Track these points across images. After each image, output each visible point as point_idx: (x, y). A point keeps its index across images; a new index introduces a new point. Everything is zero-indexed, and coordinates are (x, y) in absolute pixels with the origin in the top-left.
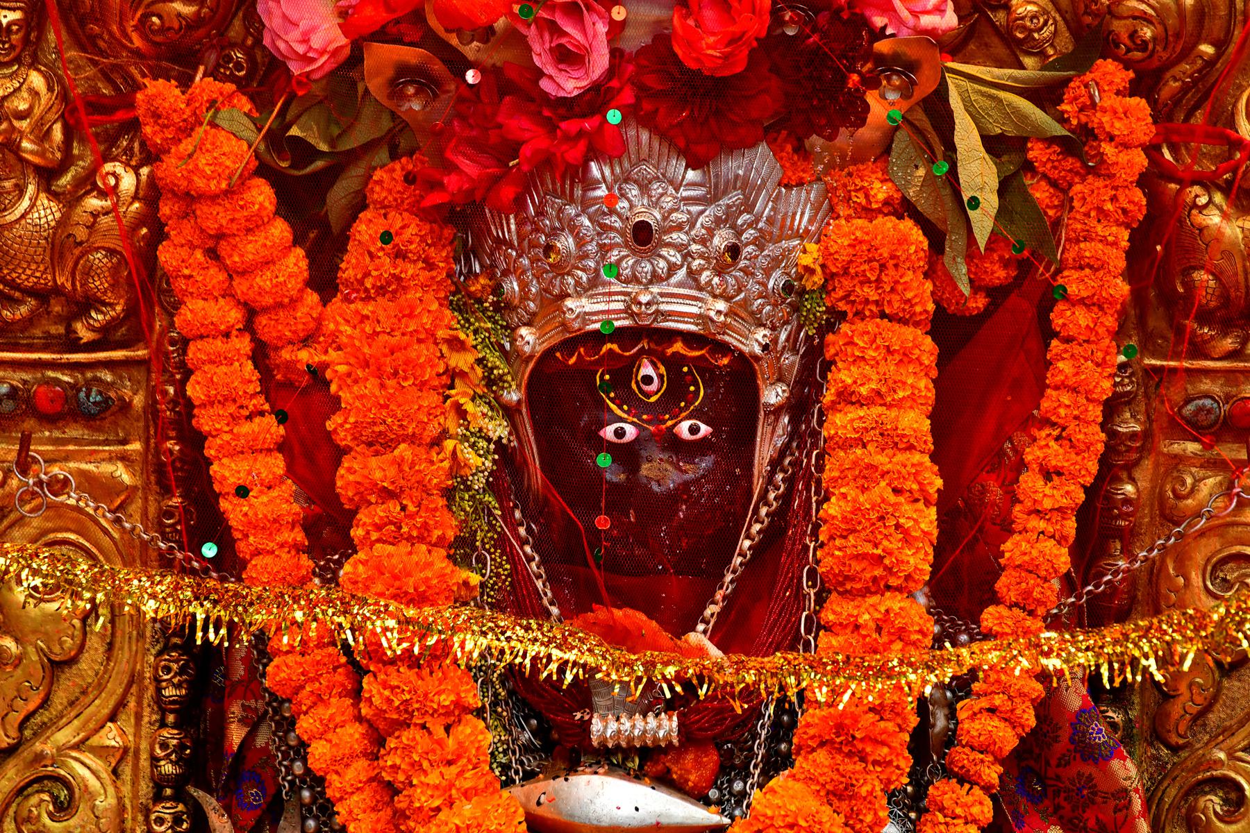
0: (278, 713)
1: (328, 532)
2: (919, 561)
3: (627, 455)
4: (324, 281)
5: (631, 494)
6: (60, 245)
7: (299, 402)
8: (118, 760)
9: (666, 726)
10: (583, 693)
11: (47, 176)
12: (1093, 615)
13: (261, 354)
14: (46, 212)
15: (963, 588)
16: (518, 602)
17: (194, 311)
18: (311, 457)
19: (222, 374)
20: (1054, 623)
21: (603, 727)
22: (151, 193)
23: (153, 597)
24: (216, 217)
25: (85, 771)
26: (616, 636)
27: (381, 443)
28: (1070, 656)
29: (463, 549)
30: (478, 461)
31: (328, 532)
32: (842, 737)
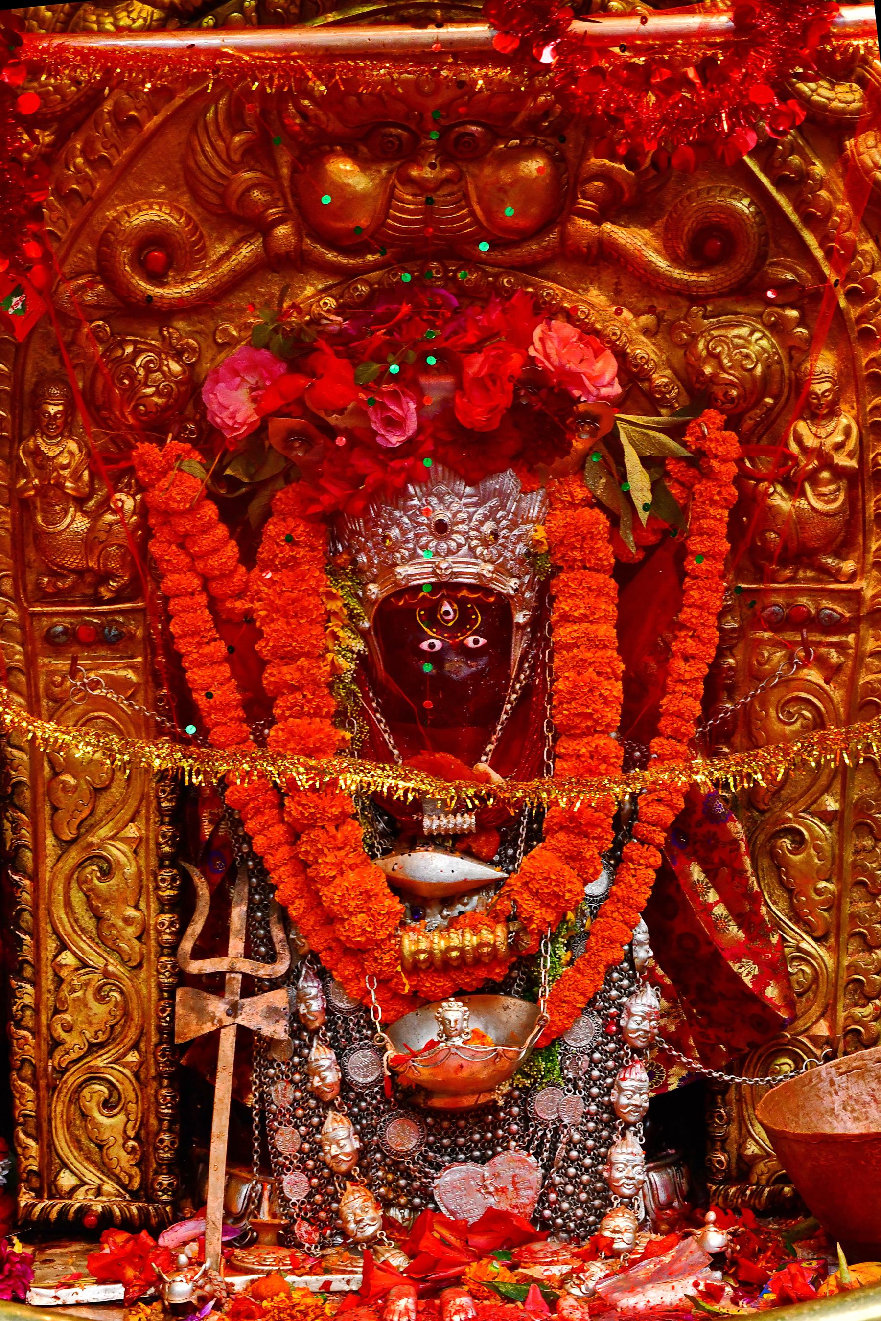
1: (258, 708)
2: (613, 715)
3: (437, 658)
5: (441, 679)
6: (90, 542)
9: (468, 821)
10: (418, 806)
11: (80, 502)
13: (213, 605)
14: (81, 524)
17: (171, 581)
19: (191, 617)
21: (430, 823)
22: (142, 510)
25: (118, 851)
26: (436, 771)
27: (289, 658)
30: (347, 666)
31: (258, 708)
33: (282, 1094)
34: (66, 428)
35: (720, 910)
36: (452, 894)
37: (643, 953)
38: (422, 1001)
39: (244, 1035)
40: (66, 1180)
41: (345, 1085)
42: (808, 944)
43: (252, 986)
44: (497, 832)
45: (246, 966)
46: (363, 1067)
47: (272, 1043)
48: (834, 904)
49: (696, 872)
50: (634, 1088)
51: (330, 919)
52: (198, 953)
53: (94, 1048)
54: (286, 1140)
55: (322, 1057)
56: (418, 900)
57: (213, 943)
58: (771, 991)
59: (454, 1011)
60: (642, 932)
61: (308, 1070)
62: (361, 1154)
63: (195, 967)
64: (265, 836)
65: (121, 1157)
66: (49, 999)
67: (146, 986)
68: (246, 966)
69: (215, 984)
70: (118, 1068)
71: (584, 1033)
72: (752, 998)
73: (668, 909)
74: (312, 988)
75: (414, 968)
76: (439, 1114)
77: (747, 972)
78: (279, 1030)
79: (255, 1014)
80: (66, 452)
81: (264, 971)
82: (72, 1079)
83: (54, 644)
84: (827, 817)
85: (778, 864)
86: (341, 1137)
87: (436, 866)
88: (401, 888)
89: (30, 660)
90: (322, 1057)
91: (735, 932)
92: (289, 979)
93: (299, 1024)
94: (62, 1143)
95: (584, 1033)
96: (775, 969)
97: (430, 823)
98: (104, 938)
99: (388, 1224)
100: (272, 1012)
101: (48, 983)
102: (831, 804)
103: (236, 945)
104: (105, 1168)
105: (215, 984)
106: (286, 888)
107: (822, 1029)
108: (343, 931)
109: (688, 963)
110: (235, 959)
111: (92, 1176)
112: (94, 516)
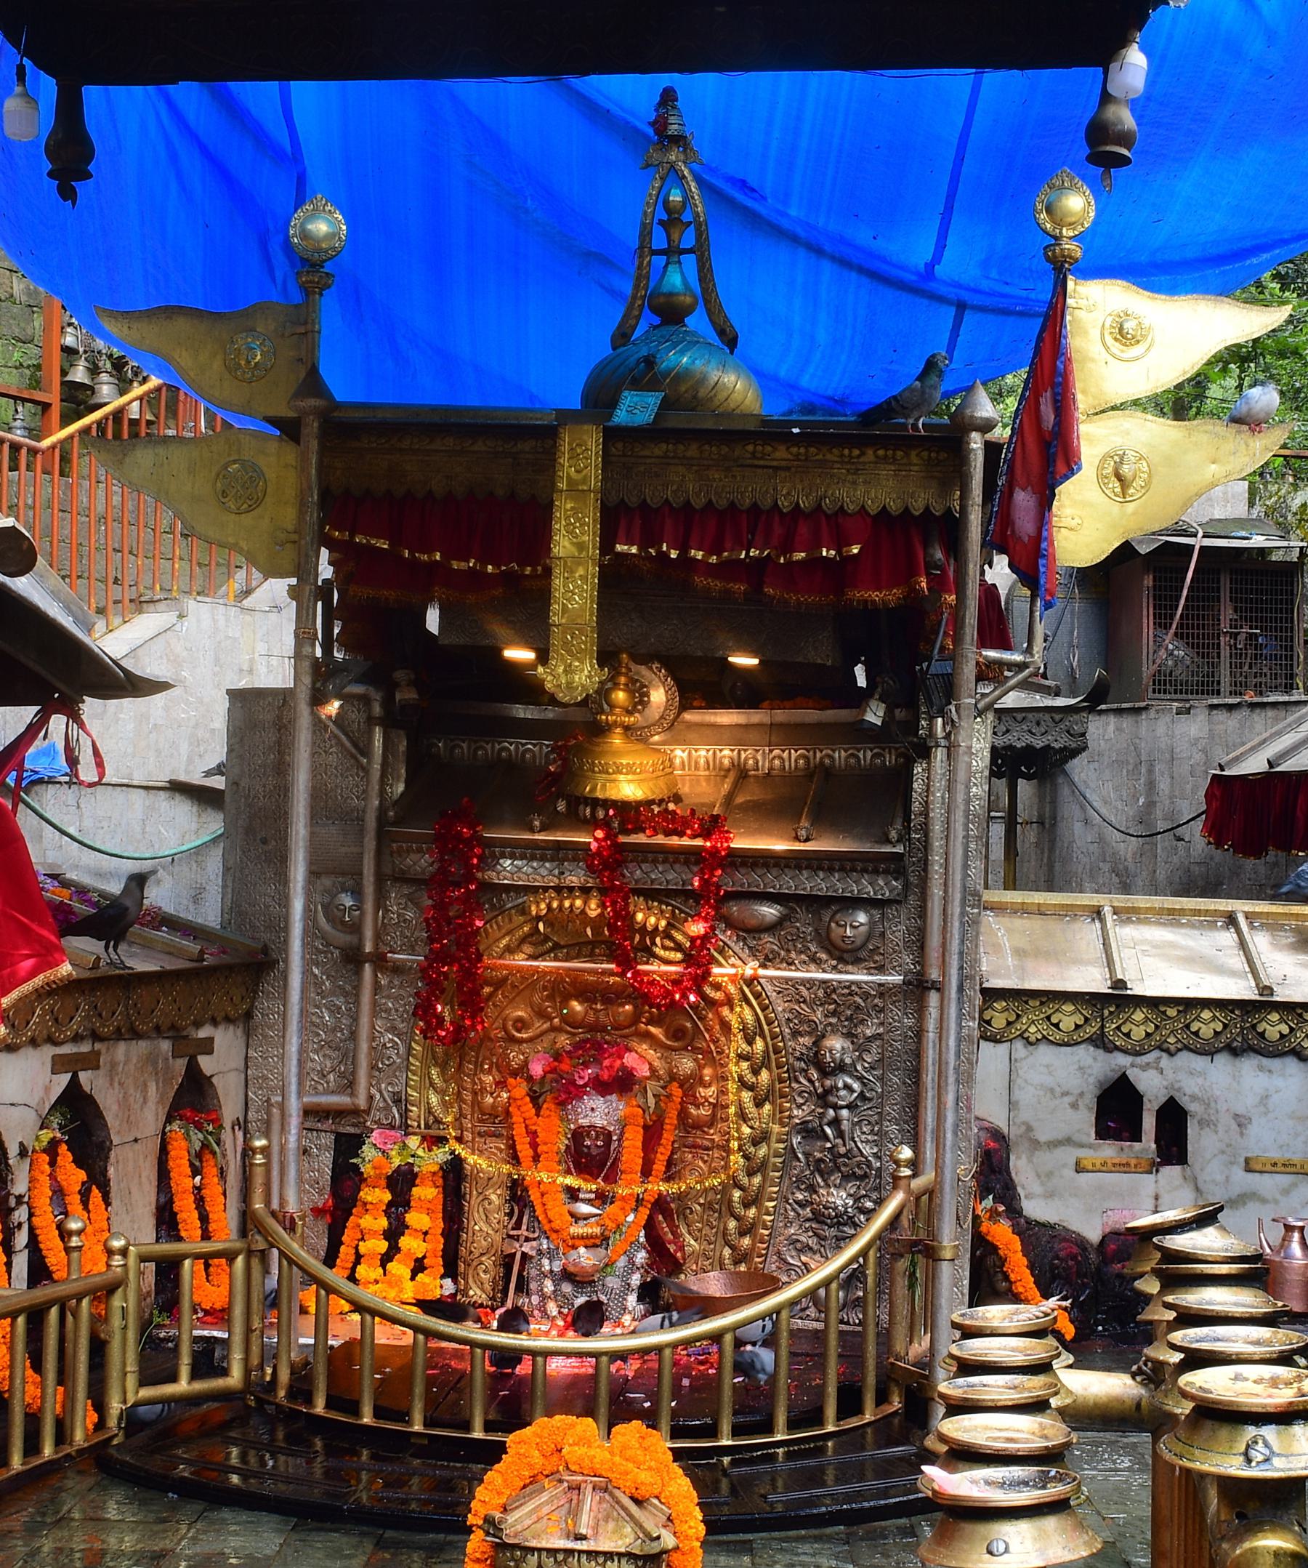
0: (526, 1190)
1: (536, 1158)
2: (639, 1168)
3: (588, 1147)
4: (538, 1115)
5: (589, 1154)
6: (493, 1106)
7: (533, 1135)
8: (499, 1196)
9: (593, 1196)
10: (579, 1190)
11: (492, 1094)
12: (668, 1179)
13: (526, 1127)
14: (491, 1100)
15: (646, 1172)
16: (568, 1172)
17: (514, 1119)
18: (534, 1145)
19: (519, 1131)
20: (662, 1180)
21: (581, 1196)
22: (509, 1098)
23: (506, 1168)
24: (519, 1103)
25: (493, 1197)
26: (585, 1180)
27: (545, 1144)
28: (663, 1187)
29: (559, 1163)
30: (563, 1148)
31: (536, 1158)
32: (623, 1198)
33: (534, 1272)
34: (489, 1072)
35: (666, 1229)
36: (586, 1217)
37: (642, 1240)
38: (574, 1247)
39: (524, 1255)
40: (471, 1293)
41: (551, 1271)
42: (692, 1242)
43: (527, 1239)
44: (602, 1198)
45: (526, 1233)
46: (557, 1267)
47: (532, 1257)
48: (700, 1230)
49: (660, 1217)
50: (636, 1280)
51: (550, 1221)
52: (513, 1229)
53: (482, 1255)
54: (533, 1286)
55: (546, 1262)
56: (577, 1218)
57: (518, 1226)
58: (679, 1255)
59: (582, 1250)
60: (642, 1233)
61: (541, 1265)
62: (554, 1291)
63: (512, 1233)
64: (534, 1195)
65: (488, 1287)
66: (470, 1239)
67: (498, 1238)
68: (526, 1233)
69: (517, 1238)
70: (488, 1261)
71: (622, 1262)
72: (673, 1257)
73: (650, 1227)
74: (545, 1241)
75: (573, 1238)
76: (579, 1282)
77: (672, 1248)
78: (533, 1253)
79: (527, 1248)
80: (488, 1079)
81: (531, 1236)
82: (475, 1263)
83: (480, 1134)
84: (700, 1205)
85: (685, 1217)
86: (549, 1286)
87: (584, 1209)
88: (572, 1215)
89: (473, 1139)
90: (546, 1262)
91: (670, 1236)
92: (539, 1237)
93: (540, 1252)
94: (470, 1281)
95: (622, 1262)
96: (682, 1248)
97: (581, 1196)
98: (488, 1222)
99: (560, 1313)
100: (532, 1248)
101: (470, 1234)
102: (702, 1201)
103: (524, 1227)
104: (483, 1290)
105: (517, 1238)
106: (539, 1211)
107: (694, 1267)
108: (553, 1225)
109: (655, 1244)
110: (523, 1231)
111: (479, 1292)
112: (495, 1098)
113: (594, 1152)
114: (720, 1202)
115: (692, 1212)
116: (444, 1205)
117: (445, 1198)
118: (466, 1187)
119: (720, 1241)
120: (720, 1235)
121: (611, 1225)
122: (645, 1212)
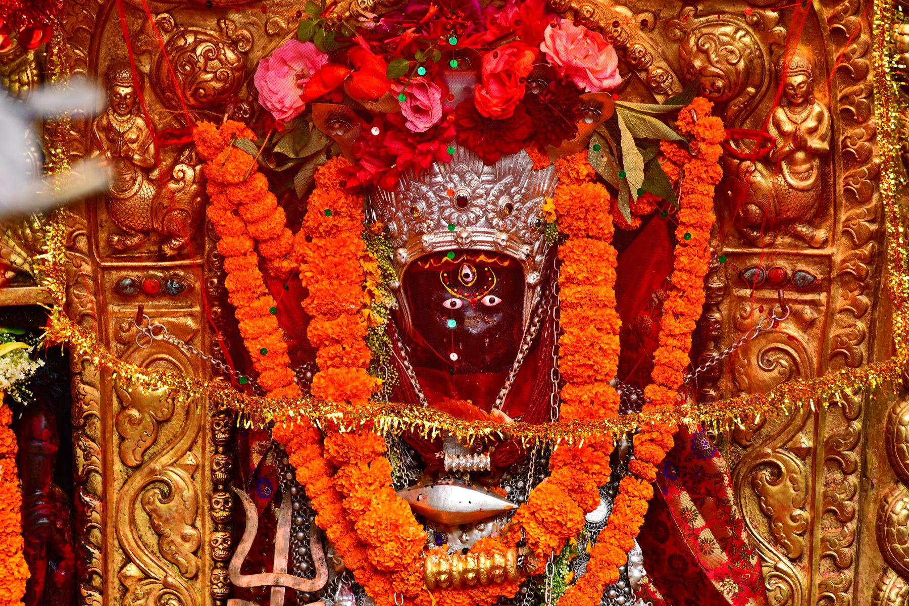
2: (611, 365)
3: (458, 315)
4: (294, 222)
5: (461, 332)
6: (156, 208)
9: (483, 461)
11: (147, 171)
13: (263, 263)
14: (148, 191)
17: (226, 243)
19: (244, 278)
21: (451, 460)
22: (202, 180)
24: (238, 194)
25: (177, 476)
26: (457, 413)
27: (331, 315)
29: (374, 366)
30: (381, 320)
31: (302, 354)
35: (707, 534)
36: (469, 522)
37: (637, 573)
42: (785, 565)
45: (288, 581)
48: (808, 529)
49: (685, 500)
51: (363, 545)
56: (439, 526)
60: (636, 555)
68: (288, 581)
81: (305, 586)
83: (122, 293)
84: (801, 453)
85: (759, 493)
87: (456, 498)
88: (424, 517)
91: (719, 555)
97: (451, 460)
101: (114, 591)
102: (806, 442)
103: (280, 562)
106: (326, 514)
112: (160, 183)
113: (476, 327)
114: (861, 441)
115: (777, 475)
116: (27, 509)
117: (27, 490)
118: (87, 452)
119: (870, 556)
120: (869, 539)
121: (547, 541)
122: (639, 494)
